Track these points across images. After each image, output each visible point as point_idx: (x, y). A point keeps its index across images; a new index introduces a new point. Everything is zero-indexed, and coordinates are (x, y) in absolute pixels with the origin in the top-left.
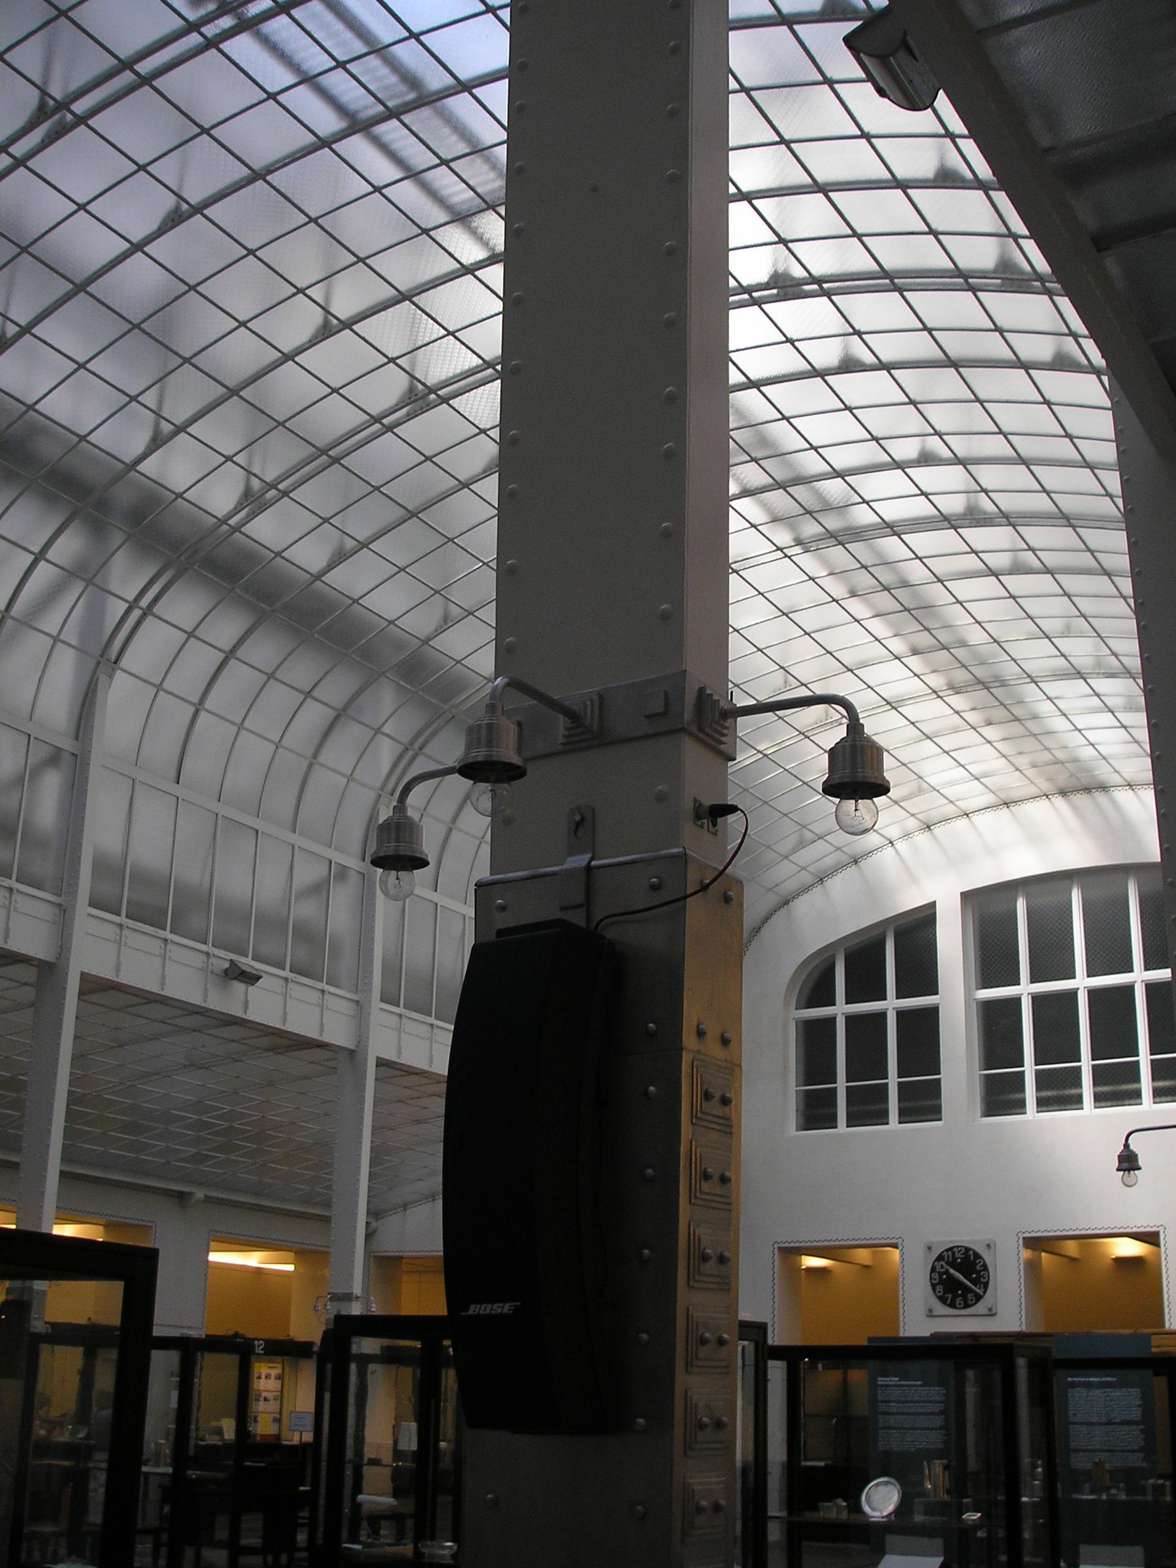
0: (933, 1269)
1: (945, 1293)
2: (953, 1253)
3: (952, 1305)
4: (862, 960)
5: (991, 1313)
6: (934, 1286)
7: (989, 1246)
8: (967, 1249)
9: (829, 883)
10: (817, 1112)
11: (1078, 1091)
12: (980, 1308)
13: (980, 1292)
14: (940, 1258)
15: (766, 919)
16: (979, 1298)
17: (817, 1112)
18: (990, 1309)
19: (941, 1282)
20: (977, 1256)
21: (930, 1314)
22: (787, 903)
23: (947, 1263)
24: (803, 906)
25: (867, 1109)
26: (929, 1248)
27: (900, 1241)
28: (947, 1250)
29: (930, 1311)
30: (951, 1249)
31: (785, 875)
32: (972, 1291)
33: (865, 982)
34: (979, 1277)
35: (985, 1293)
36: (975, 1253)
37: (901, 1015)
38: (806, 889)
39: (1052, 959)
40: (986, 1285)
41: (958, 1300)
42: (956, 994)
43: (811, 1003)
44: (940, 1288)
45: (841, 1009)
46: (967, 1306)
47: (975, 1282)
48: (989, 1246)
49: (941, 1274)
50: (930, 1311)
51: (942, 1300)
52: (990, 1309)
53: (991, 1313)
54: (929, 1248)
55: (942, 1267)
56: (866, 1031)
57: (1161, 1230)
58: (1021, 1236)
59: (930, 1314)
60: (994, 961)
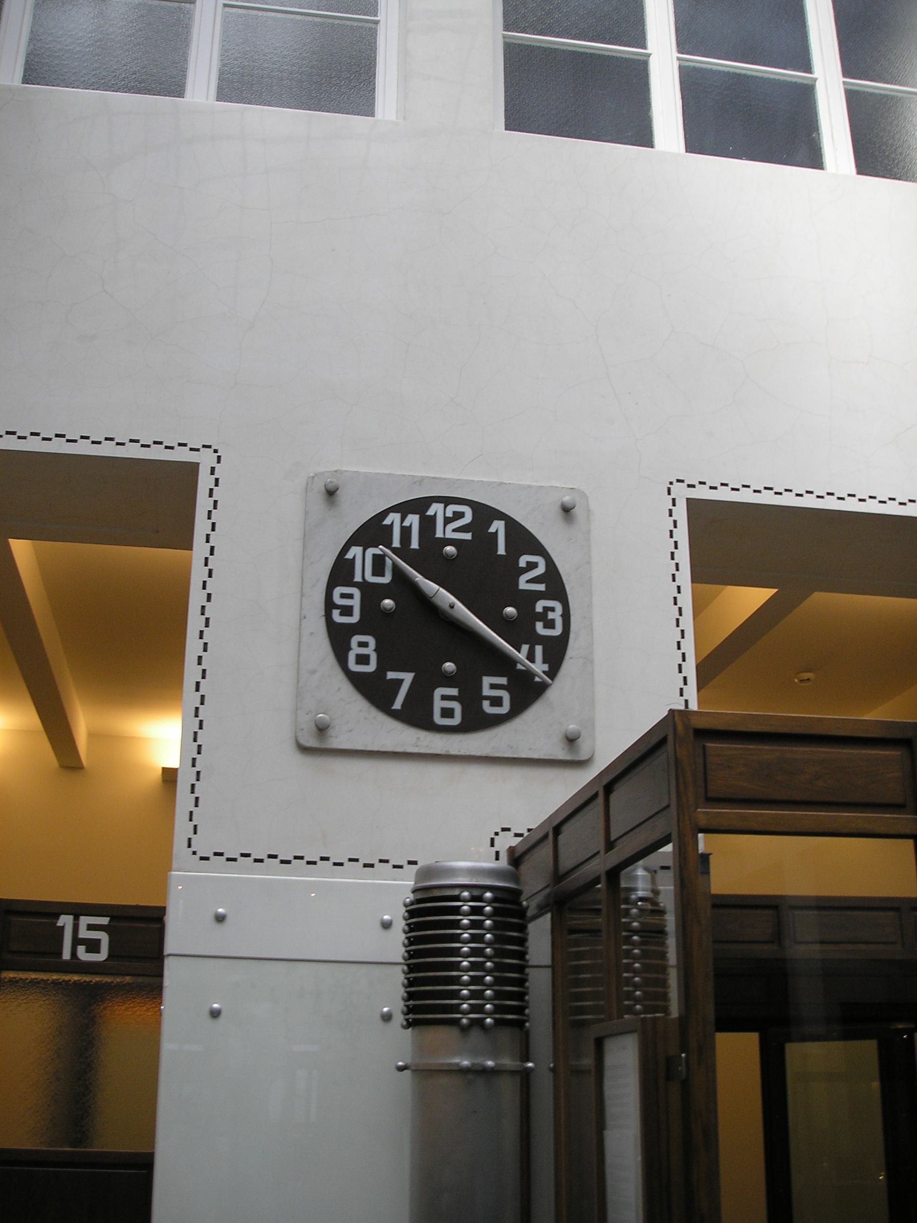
0: (341, 572)
2: (428, 524)
3: (417, 715)
6: (339, 638)
7: (567, 510)
8: (484, 514)
13: (539, 667)
14: (372, 532)
16: (527, 691)
18: (571, 741)
20: (522, 539)
23: (404, 552)
26: (331, 493)
28: (404, 508)
29: (322, 730)
30: (419, 506)
32: (504, 664)
34: (528, 616)
35: (553, 673)
36: (513, 526)
40: (556, 652)
41: (442, 698)
44: (364, 645)
46: (474, 721)
47: (520, 632)
50: (322, 730)
51: (374, 689)
52: (571, 741)
54: (331, 493)
55: (379, 565)
58: (682, 493)
59: (318, 745)
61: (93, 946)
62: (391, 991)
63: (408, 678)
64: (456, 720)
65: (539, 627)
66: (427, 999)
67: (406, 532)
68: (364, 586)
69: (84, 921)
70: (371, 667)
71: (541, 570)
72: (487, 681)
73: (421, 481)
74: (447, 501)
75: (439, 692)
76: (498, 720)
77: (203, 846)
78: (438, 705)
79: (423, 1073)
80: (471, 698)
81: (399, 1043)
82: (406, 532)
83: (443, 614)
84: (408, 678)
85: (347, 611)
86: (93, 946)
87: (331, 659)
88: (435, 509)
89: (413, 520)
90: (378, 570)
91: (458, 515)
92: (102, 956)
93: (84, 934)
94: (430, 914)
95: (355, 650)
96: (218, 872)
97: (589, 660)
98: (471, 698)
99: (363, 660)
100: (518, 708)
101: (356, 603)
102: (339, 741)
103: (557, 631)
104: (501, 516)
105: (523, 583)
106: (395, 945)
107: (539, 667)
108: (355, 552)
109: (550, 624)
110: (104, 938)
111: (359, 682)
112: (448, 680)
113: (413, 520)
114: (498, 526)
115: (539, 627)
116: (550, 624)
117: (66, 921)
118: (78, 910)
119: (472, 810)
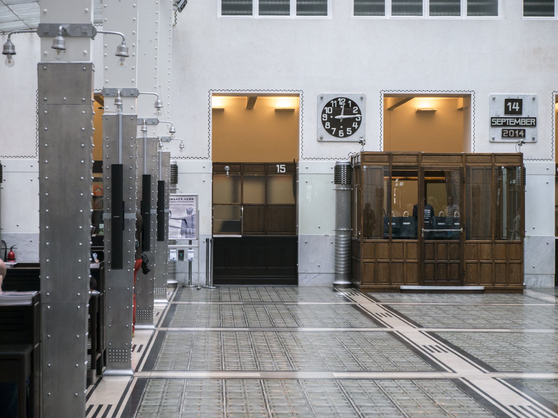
0: (324, 112)
1: (331, 127)
2: (338, 102)
3: (336, 135)
6: (324, 123)
7: (362, 98)
8: (347, 100)
11: (420, 4)
12: (355, 137)
14: (329, 105)
16: (354, 130)
19: (329, 120)
21: (321, 140)
26: (322, 98)
27: (301, 93)
28: (334, 100)
29: (321, 138)
30: (336, 99)
35: (358, 128)
36: (352, 102)
40: (359, 123)
41: (341, 132)
44: (328, 124)
46: (346, 135)
48: (362, 98)
49: (329, 115)
51: (330, 131)
54: (322, 98)
57: (472, 93)
58: (383, 93)
59: (321, 140)
61: (283, 170)
62: (332, 178)
63: (335, 129)
64: (343, 135)
65: (357, 119)
66: (337, 180)
67: (334, 104)
68: (328, 114)
69: (281, 166)
70: (329, 128)
71: (357, 109)
72: (348, 129)
73: (337, 95)
74: (341, 98)
75: (340, 131)
76: (349, 135)
77: (304, 157)
78: (340, 133)
79: (337, 190)
80: (345, 132)
81: (334, 186)
82: (334, 104)
83: (341, 117)
84: (335, 129)
85: (325, 118)
86: (283, 170)
87: (323, 126)
88: (339, 100)
89: (335, 102)
90: (330, 111)
91: (343, 100)
92: (284, 172)
93: (281, 168)
94: (338, 168)
95: (326, 125)
96: (306, 161)
97: (365, 124)
98: (345, 132)
99: (328, 126)
100: (353, 133)
101: (326, 117)
102: (324, 140)
103: (359, 120)
104: (350, 100)
105: (354, 112)
106: (333, 171)
107: (356, 126)
108: (326, 108)
109: (358, 119)
110: (284, 168)
111: (327, 130)
112: (341, 129)
113: (335, 102)
114: (350, 102)
115: (357, 119)
116: (358, 119)
117: (278, 166)
118: (280, 164)
119: (344, 151)
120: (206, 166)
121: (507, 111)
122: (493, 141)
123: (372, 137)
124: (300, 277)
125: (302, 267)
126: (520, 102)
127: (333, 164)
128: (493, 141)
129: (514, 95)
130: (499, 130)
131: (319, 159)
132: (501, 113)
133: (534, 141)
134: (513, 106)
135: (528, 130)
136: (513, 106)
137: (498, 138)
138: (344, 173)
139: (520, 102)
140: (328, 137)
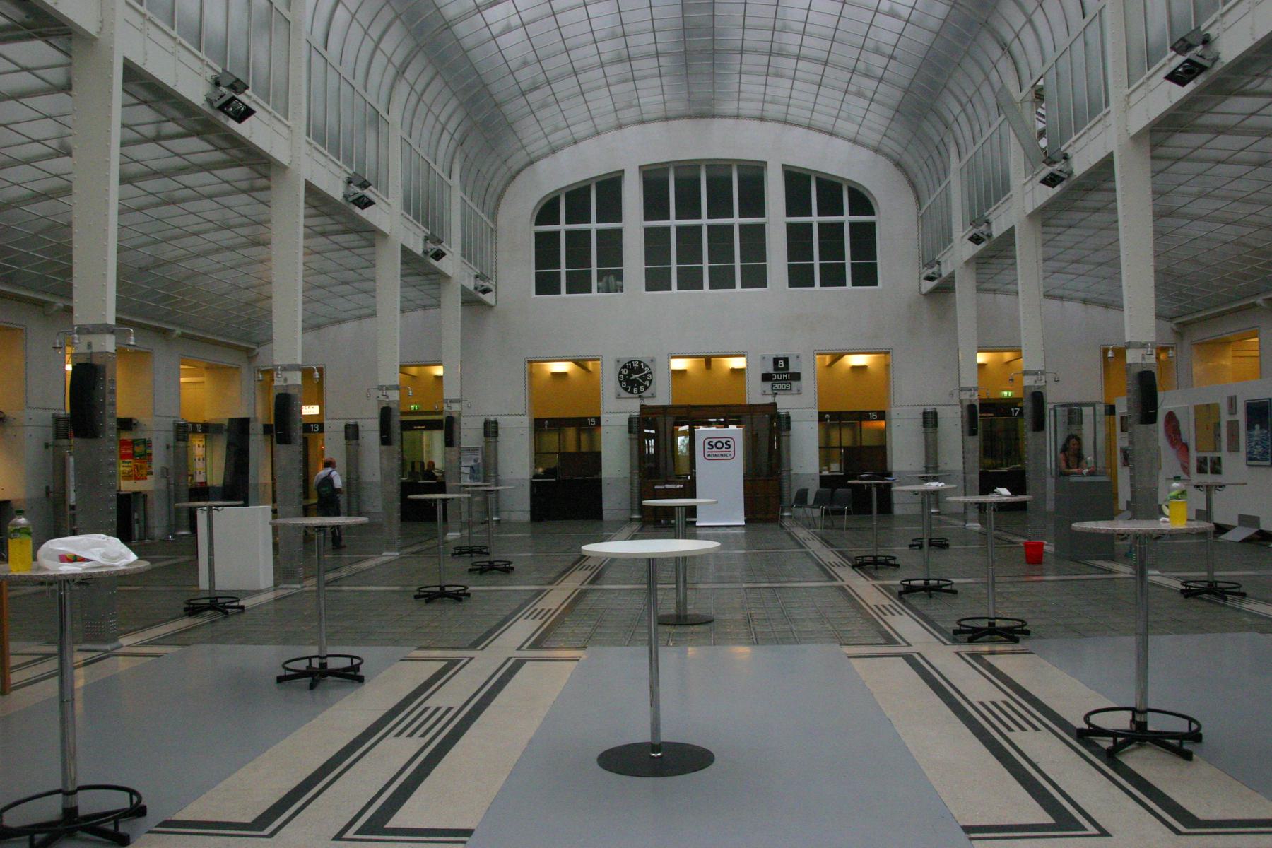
3: (631, 392)
4: (577, 199)
5: (653, 396)
9: (558, 154)
10: (546, 285)
14: (624, 367)
15: (518, 172)
16: (646, 388)
17: (546, 285)
21: (618, 396)
22: (531, 163)
24: (542, 165)
25: (579, 284)
31: (539, 146)
33: (578, 211)
37: (599, 232)
38: (544, 156)
39: (688, 207)
42: (633, 223)
43: (539, 222)
45: (563, 227)
51: (626, 389)
53: (653, 396)
56: (578, 241)
59: (618, 396)
60: (654, 205)
62: (626, 429)
66: (630, 431)
81: (627, 435)
83: (635, 376)
94: (630, 420)
120: (526, 422)
121: (776, 368)
122: (764, 393)
123: (661, 395)
124: (605, 513)
125: (605, 505)
126: (786, 360)
127: (626, 416)
128: (764, 393)
129: (781, 354)
130: (769, 384)
131: (616, 412)
132: (770, 370)
133: (799, 392)
134: (781, 363)
135: (794, 384)
136: (781, 363)
137: (769, 391)
138: (635, 423)
139: (786, 360)
140: (624, 394)
